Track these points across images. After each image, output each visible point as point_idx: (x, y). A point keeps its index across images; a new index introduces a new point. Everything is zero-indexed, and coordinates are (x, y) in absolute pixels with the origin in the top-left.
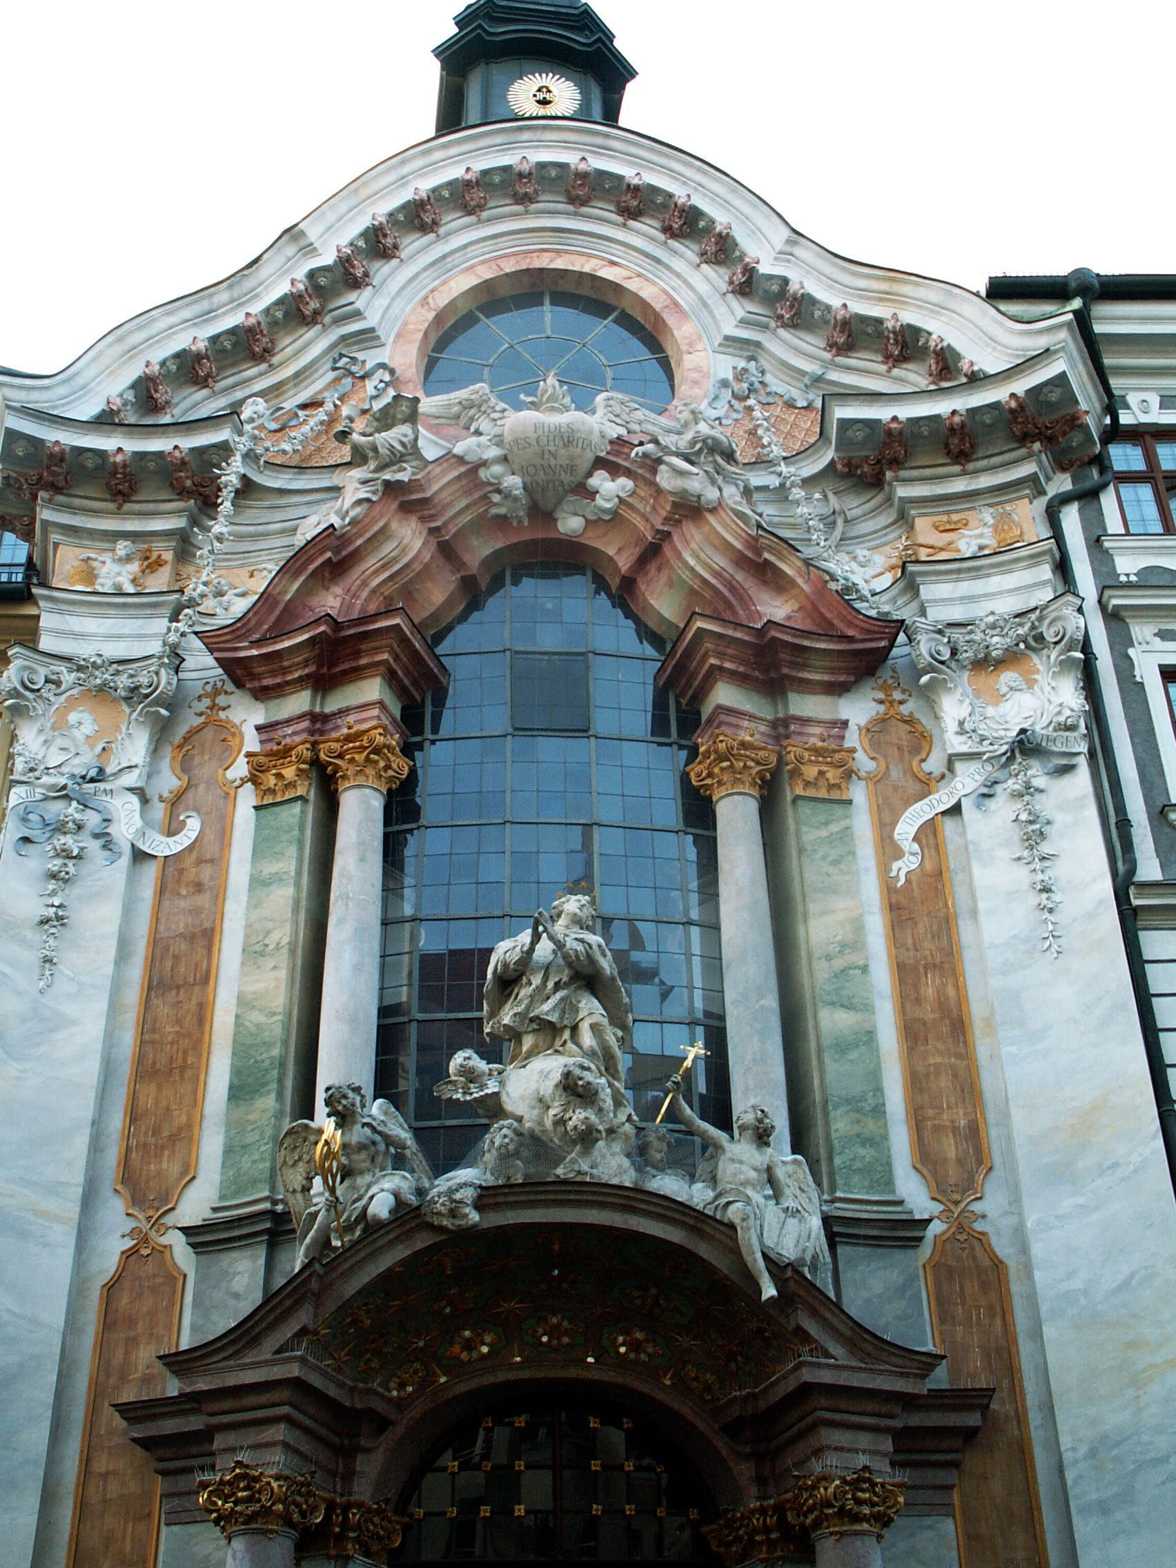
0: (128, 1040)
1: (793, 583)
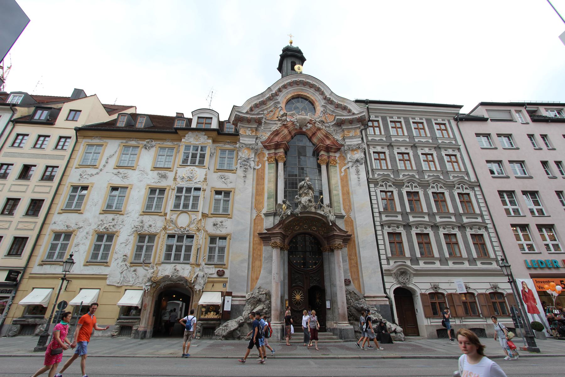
0: (254, 191)
1: (331, 139)
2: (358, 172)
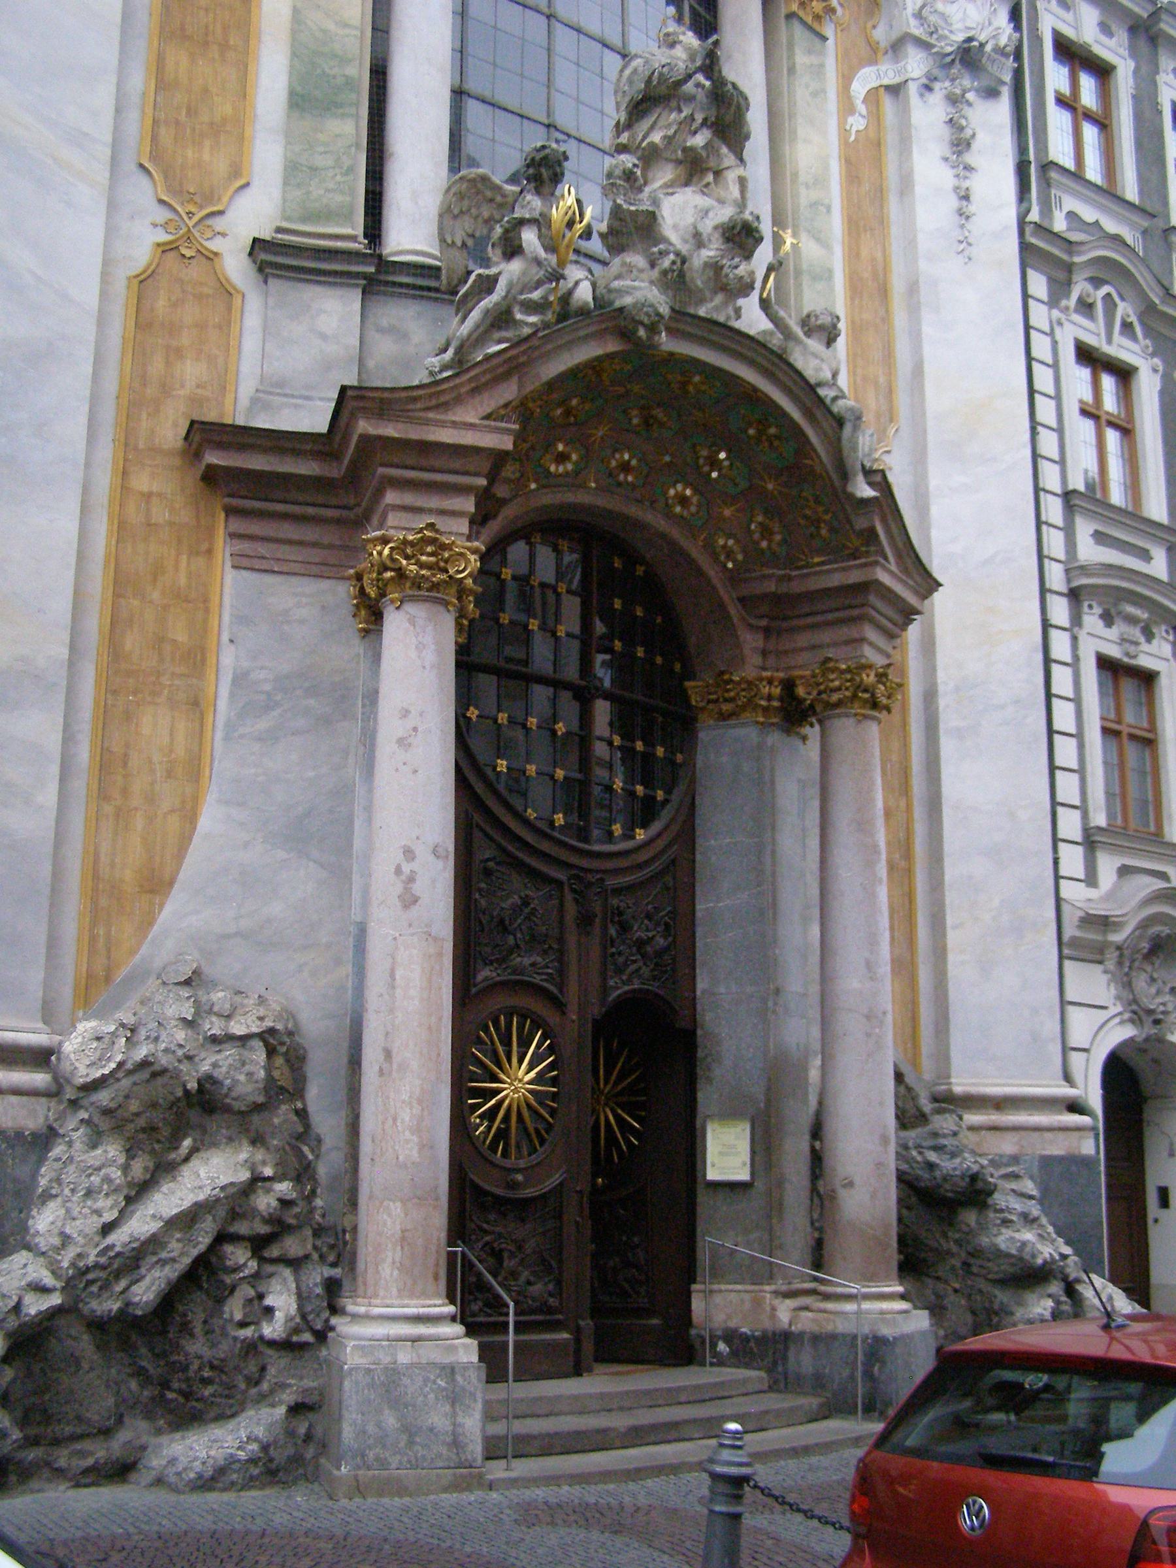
2: (961, 144)
